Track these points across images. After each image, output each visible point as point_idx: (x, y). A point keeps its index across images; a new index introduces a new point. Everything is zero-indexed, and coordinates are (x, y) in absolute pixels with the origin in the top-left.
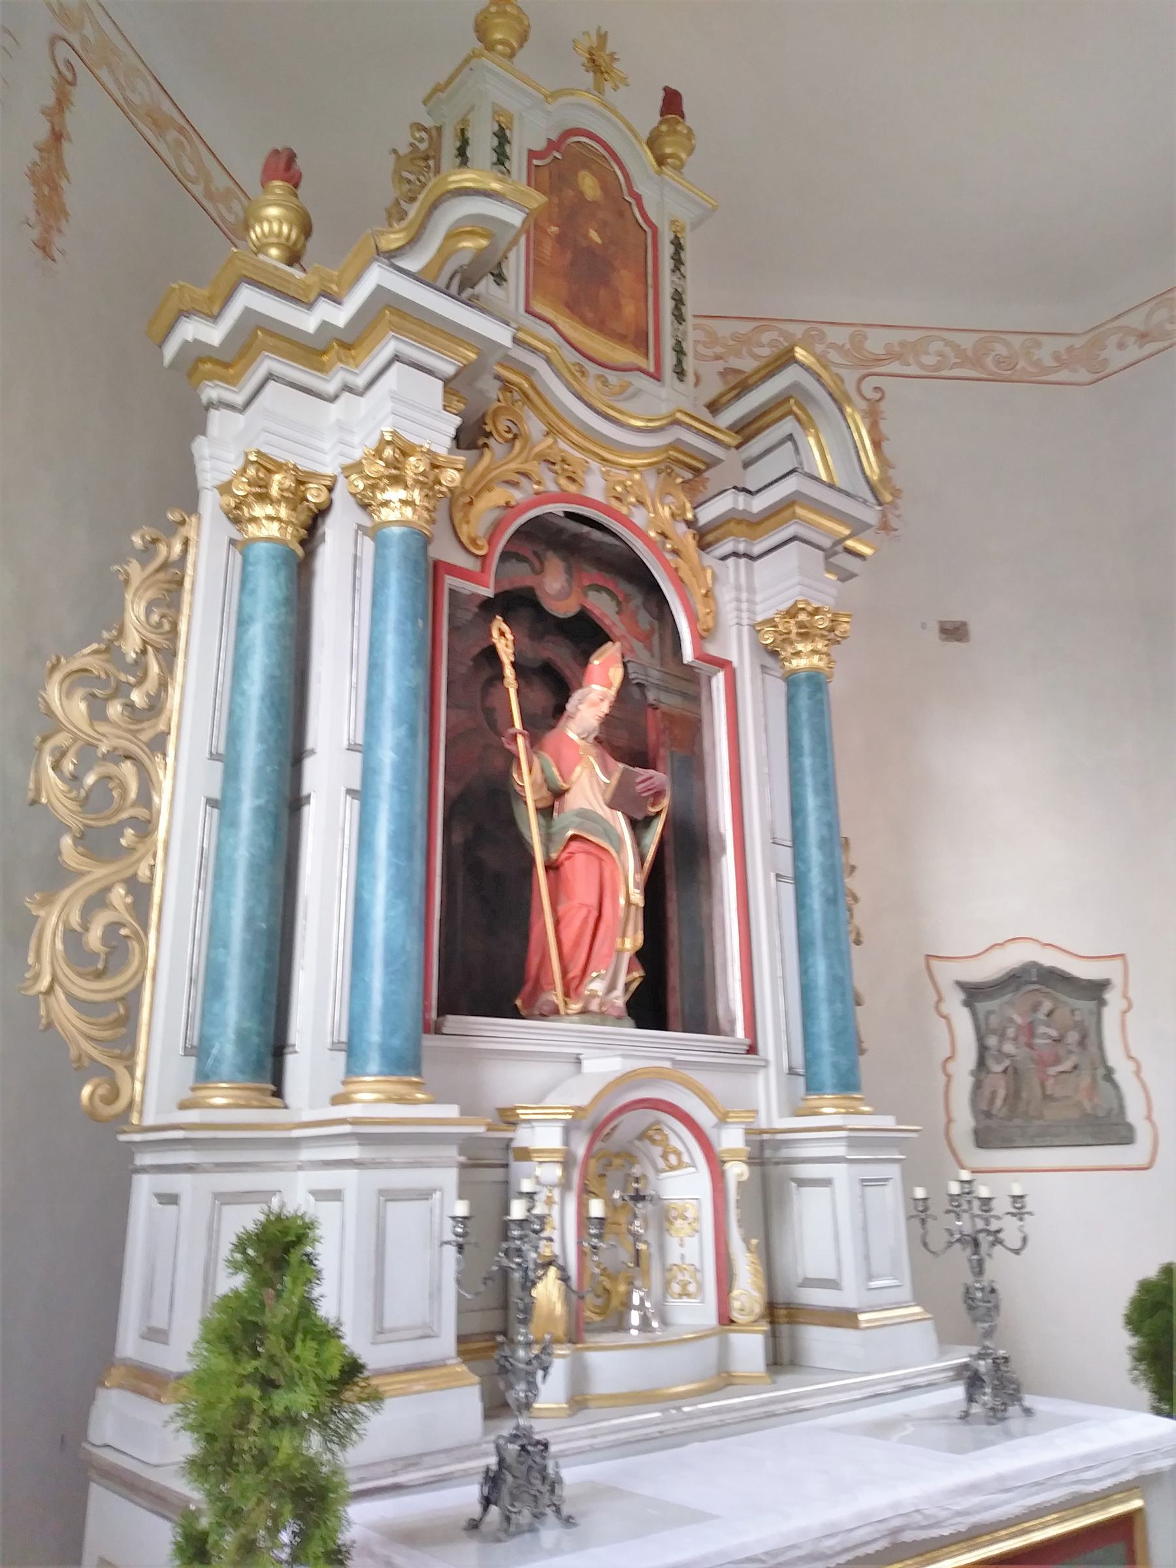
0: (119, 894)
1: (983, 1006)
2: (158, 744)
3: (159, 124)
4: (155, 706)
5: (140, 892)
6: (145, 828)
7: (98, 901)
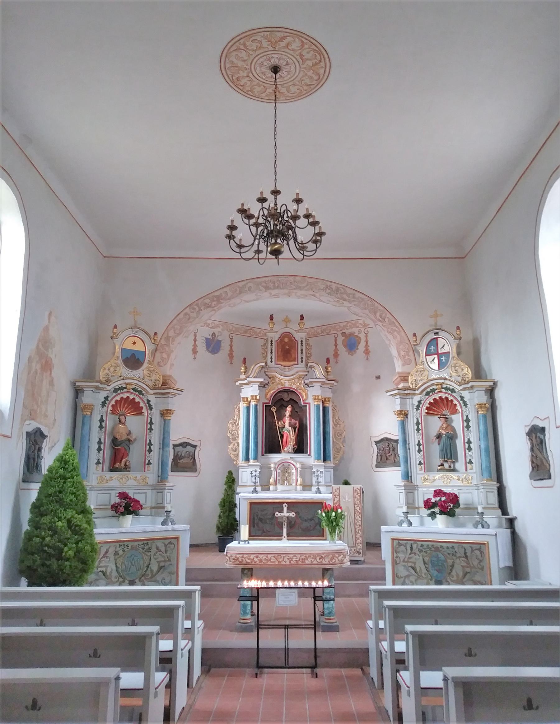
0: (236, 444)
1: (378, 445)
2: (239, 428)
3: (246, 332)
4: (238, 424)
5: (238, 443)
6: (238, 437)
7: (234, 445)
